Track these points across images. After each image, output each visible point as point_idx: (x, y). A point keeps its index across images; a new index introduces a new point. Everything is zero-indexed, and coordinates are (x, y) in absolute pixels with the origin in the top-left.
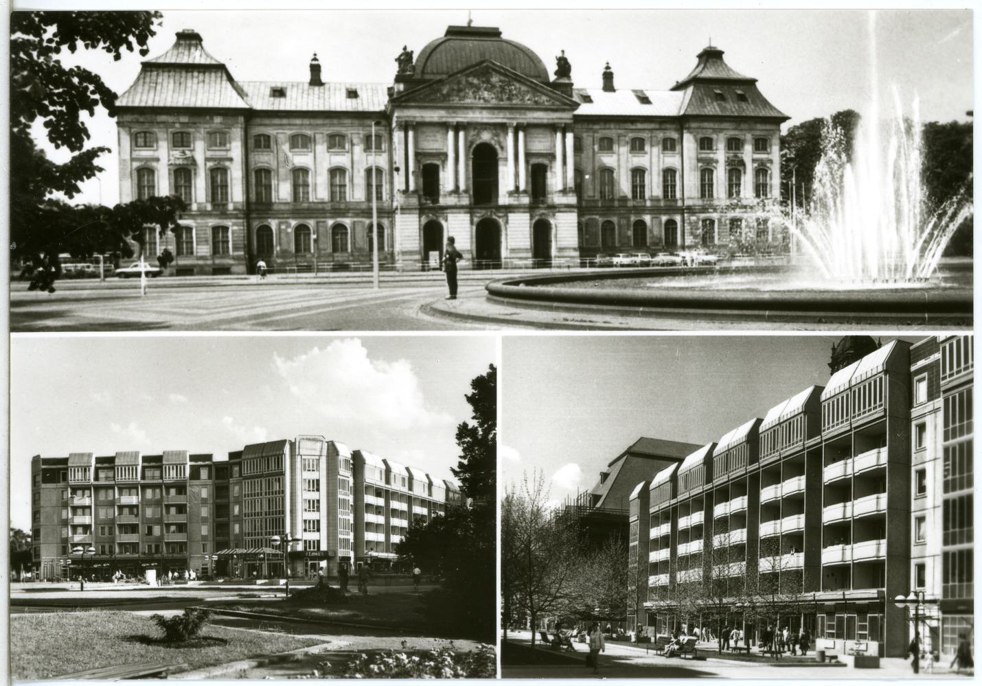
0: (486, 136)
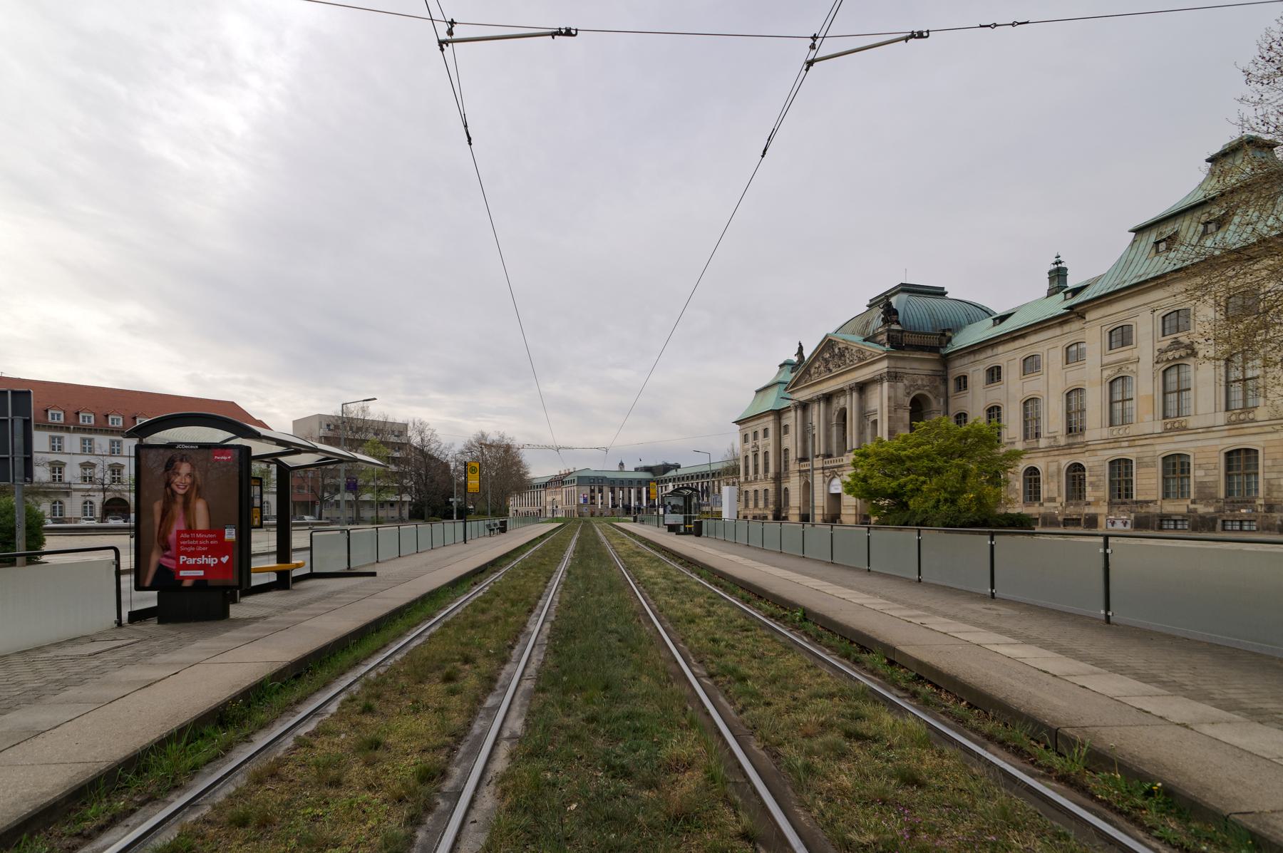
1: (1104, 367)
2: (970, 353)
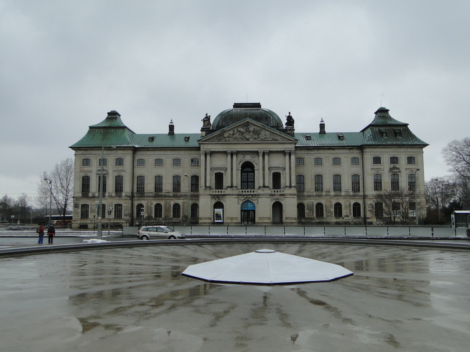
0: (248, 158)
2: (306, 149)
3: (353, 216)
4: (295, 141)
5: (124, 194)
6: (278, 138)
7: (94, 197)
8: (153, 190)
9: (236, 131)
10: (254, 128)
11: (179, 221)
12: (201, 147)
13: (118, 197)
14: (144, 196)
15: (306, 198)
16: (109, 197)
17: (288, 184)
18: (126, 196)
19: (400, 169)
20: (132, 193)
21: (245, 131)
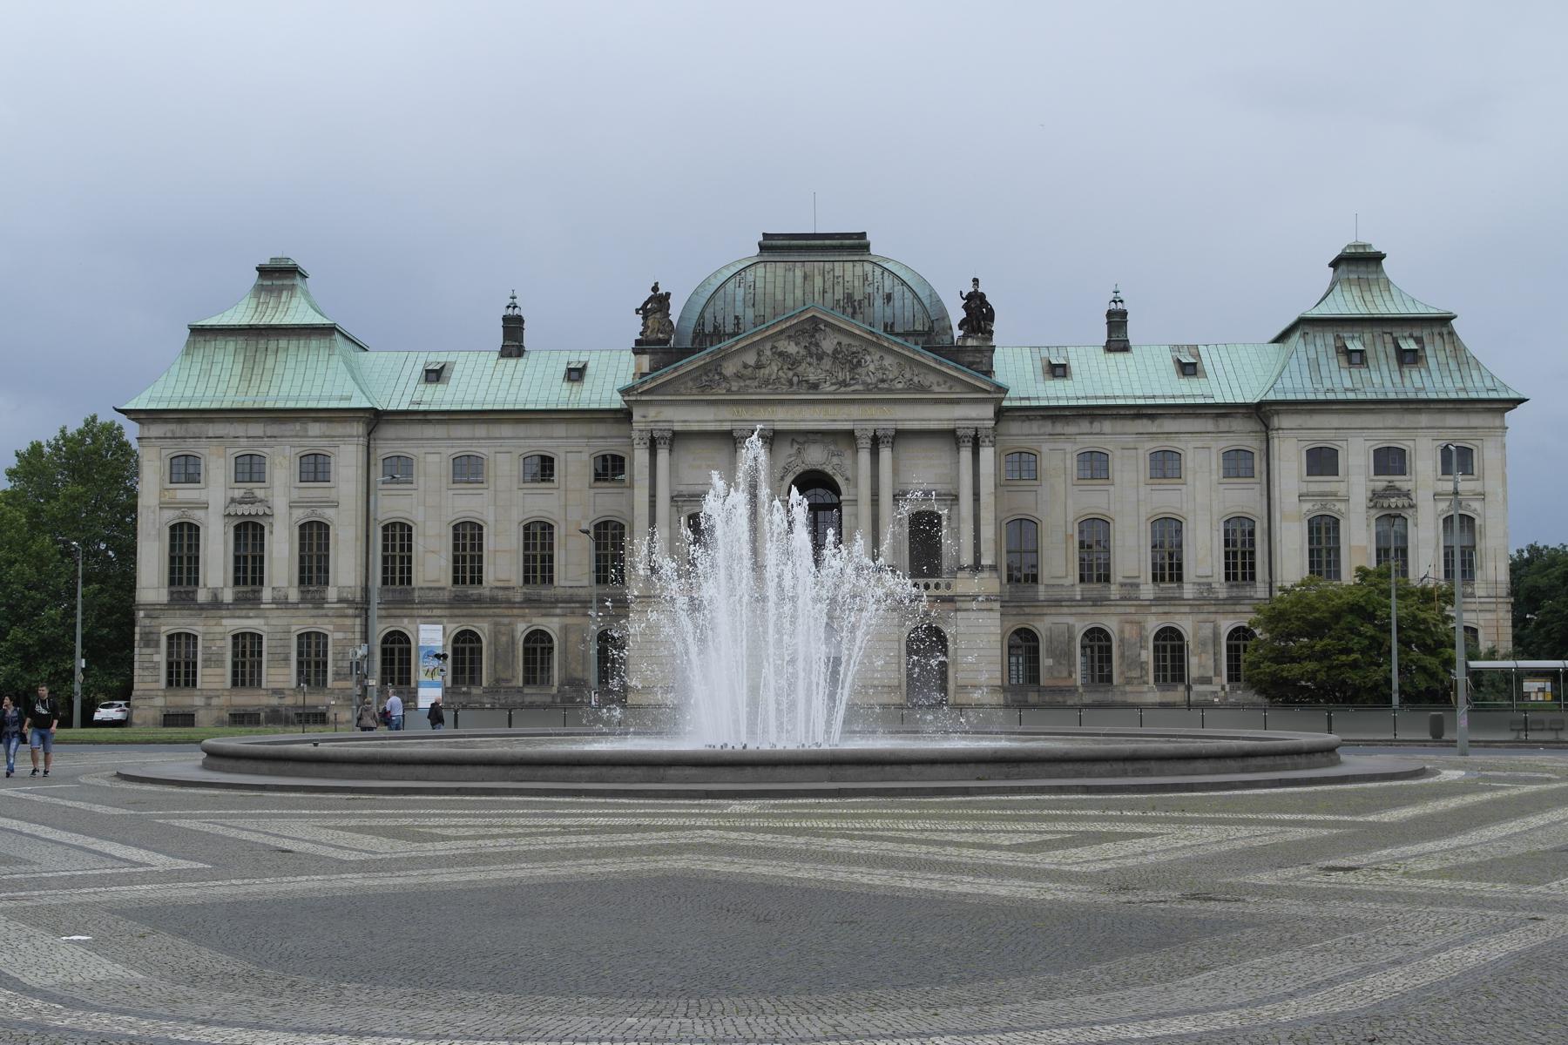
1: (1302, 497)
2: (1044, 418)
3: (1230, 679)
4: (995, 392)
5: (332, 593)
6: (931, 379)
7: (216, 604)
8: (446, 579)
9: (768, 353)
10: (839, 343)
11: (549, 699)
12: (636, 417)
13: (310, 606)
14: (412, 602)
15: (1046, 610)
16: (274, 606)
17: (967, 559)
18: (340, 601)
19: (1413, 495)
20: (366, 590)
21: (803, 352)
